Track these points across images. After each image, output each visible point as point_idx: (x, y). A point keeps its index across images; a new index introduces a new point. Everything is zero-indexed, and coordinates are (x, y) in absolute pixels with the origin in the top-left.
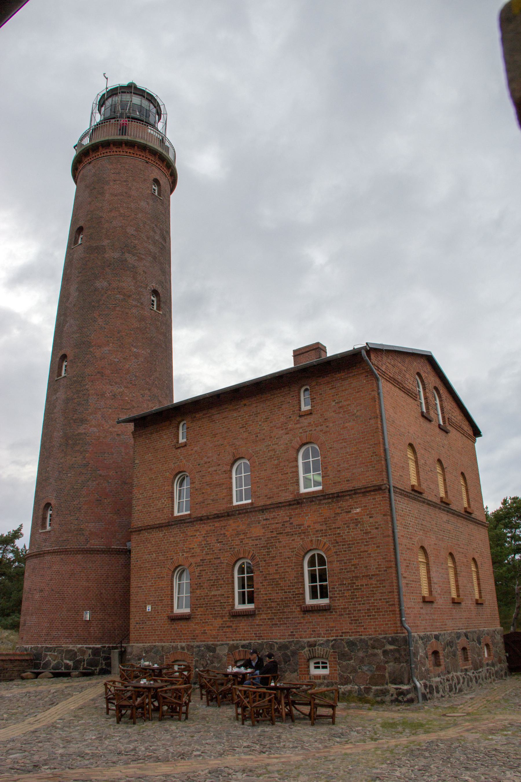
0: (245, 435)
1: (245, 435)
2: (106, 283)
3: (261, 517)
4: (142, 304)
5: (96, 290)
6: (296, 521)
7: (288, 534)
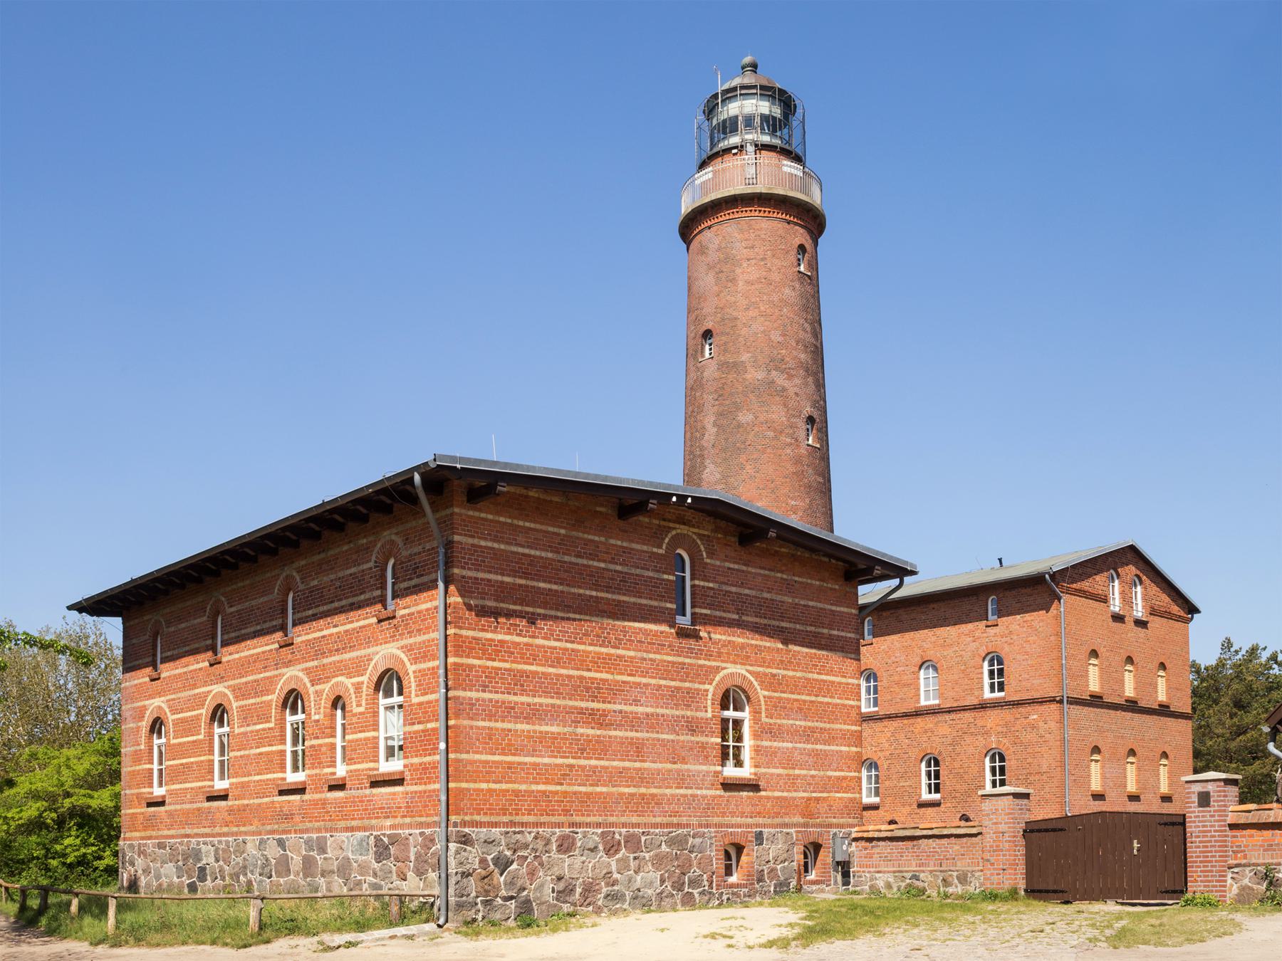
0: (934, 639)
1: (934, 639)
2: (751, 416)
3: (947, 717)
4: (797, 440)
5: (739, 426)
6: (980, 723)
7: (972, 734)
